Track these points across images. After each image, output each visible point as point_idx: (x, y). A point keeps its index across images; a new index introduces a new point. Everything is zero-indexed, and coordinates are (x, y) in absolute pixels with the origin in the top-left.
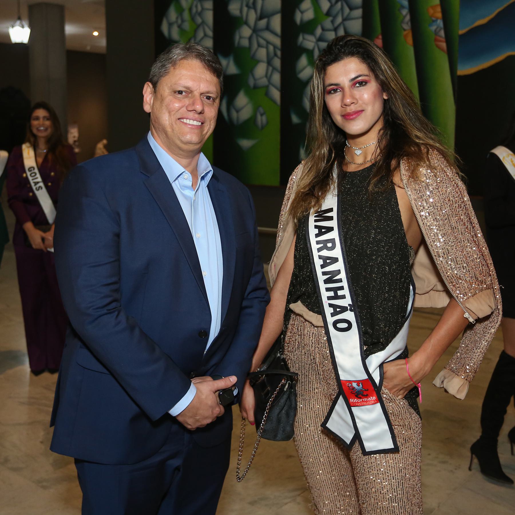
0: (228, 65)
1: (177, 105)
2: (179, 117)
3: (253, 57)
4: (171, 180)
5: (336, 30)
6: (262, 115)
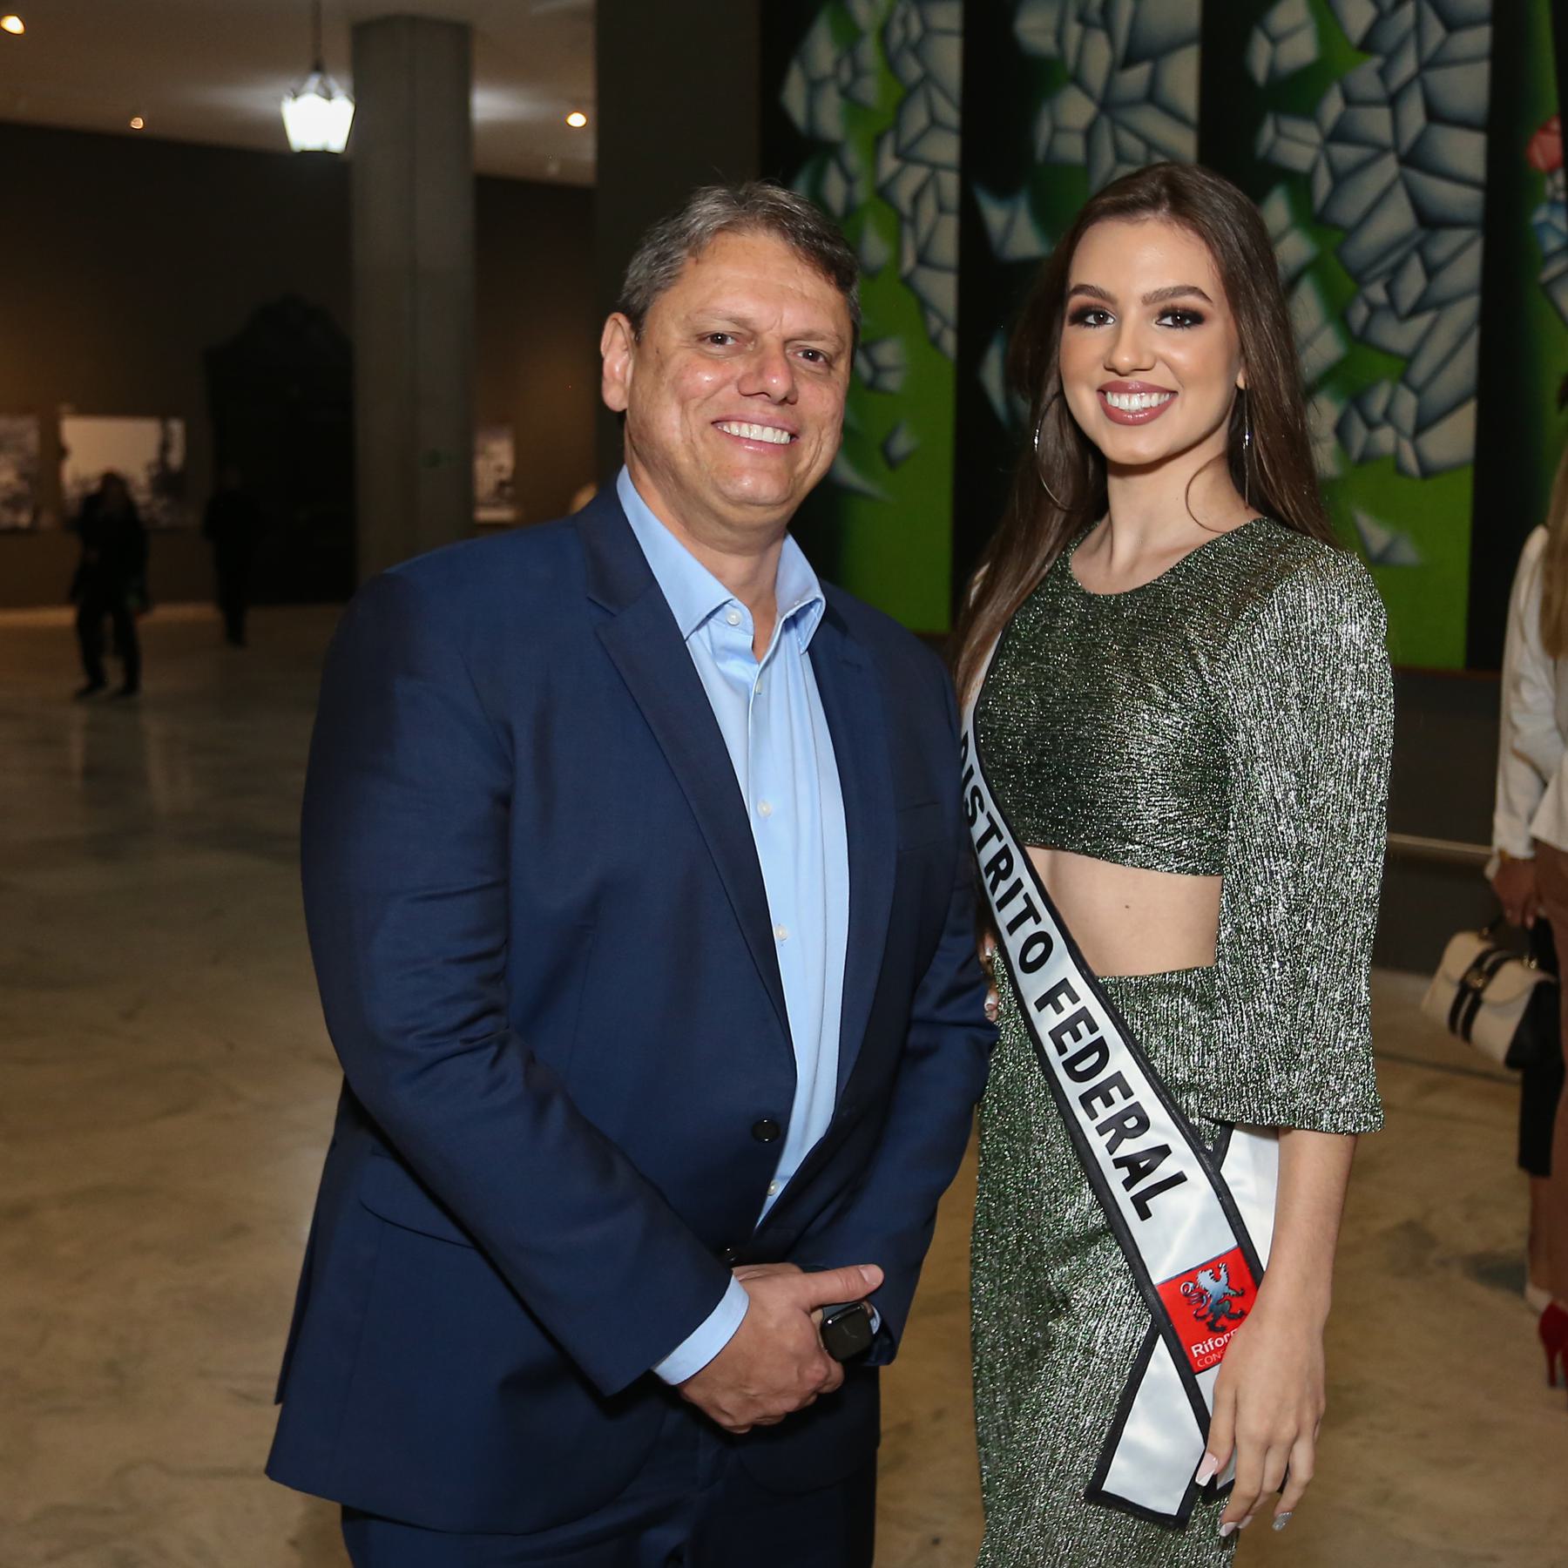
0: (1010, 224)
1: (707, 378)
2: (713, 417)
4: (685, 626)
5: (1393, 101)
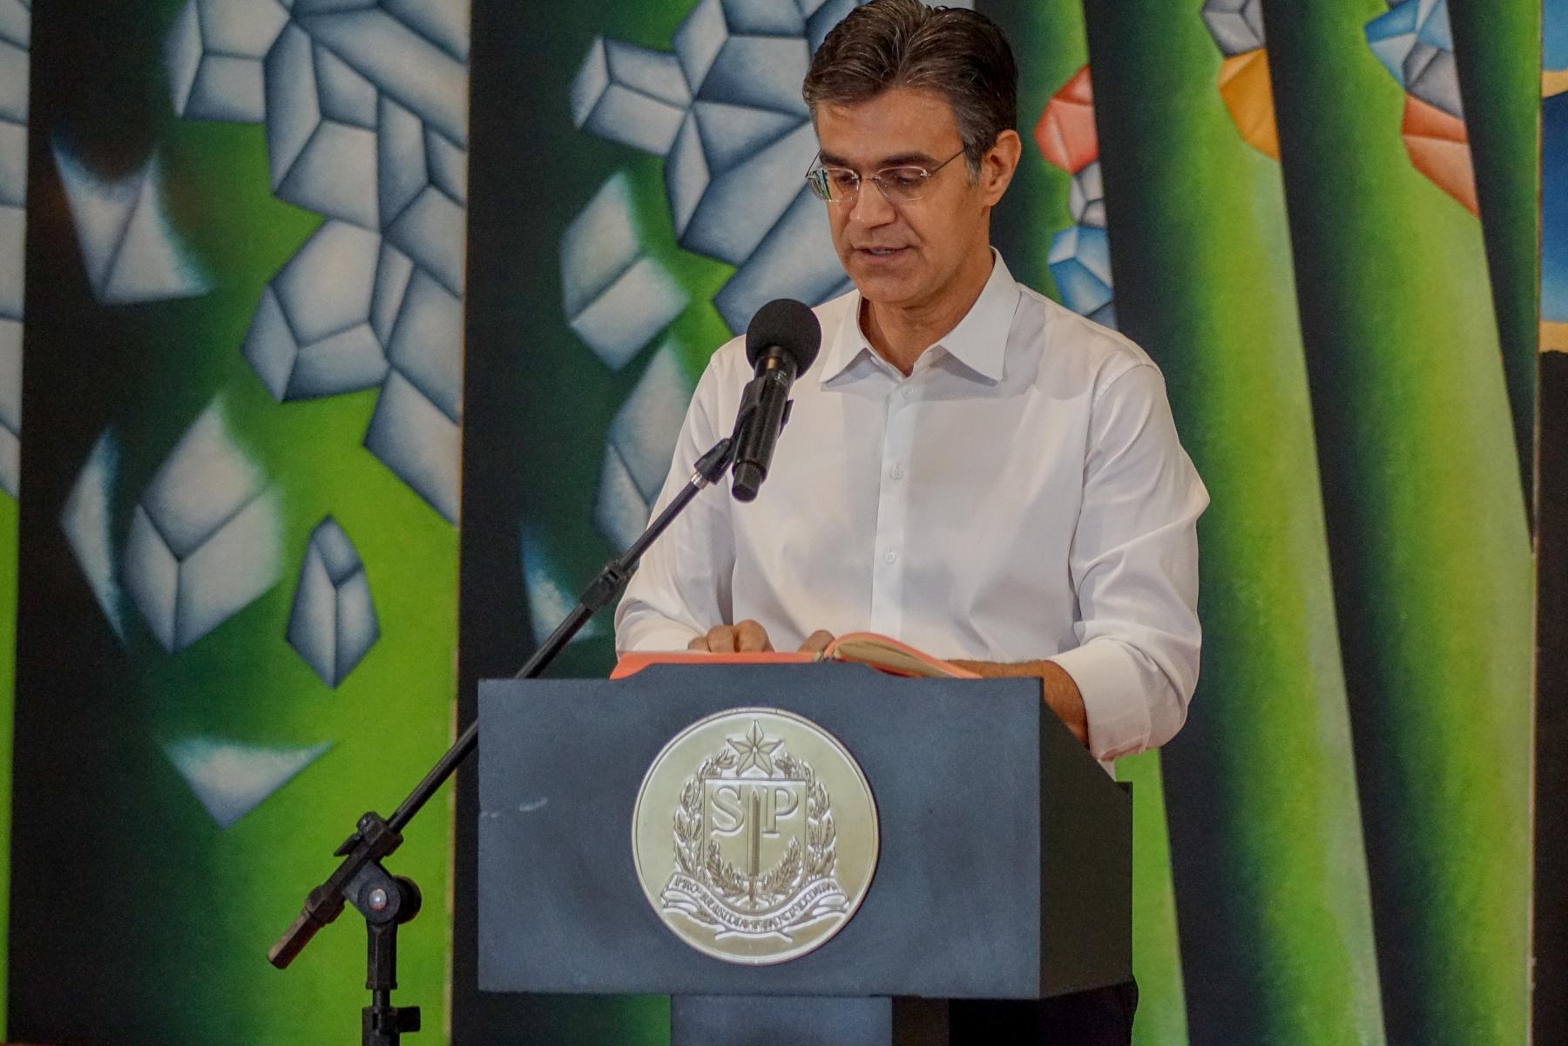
0: (124, 229)
3: (286, 190)
6: (338, 581)
